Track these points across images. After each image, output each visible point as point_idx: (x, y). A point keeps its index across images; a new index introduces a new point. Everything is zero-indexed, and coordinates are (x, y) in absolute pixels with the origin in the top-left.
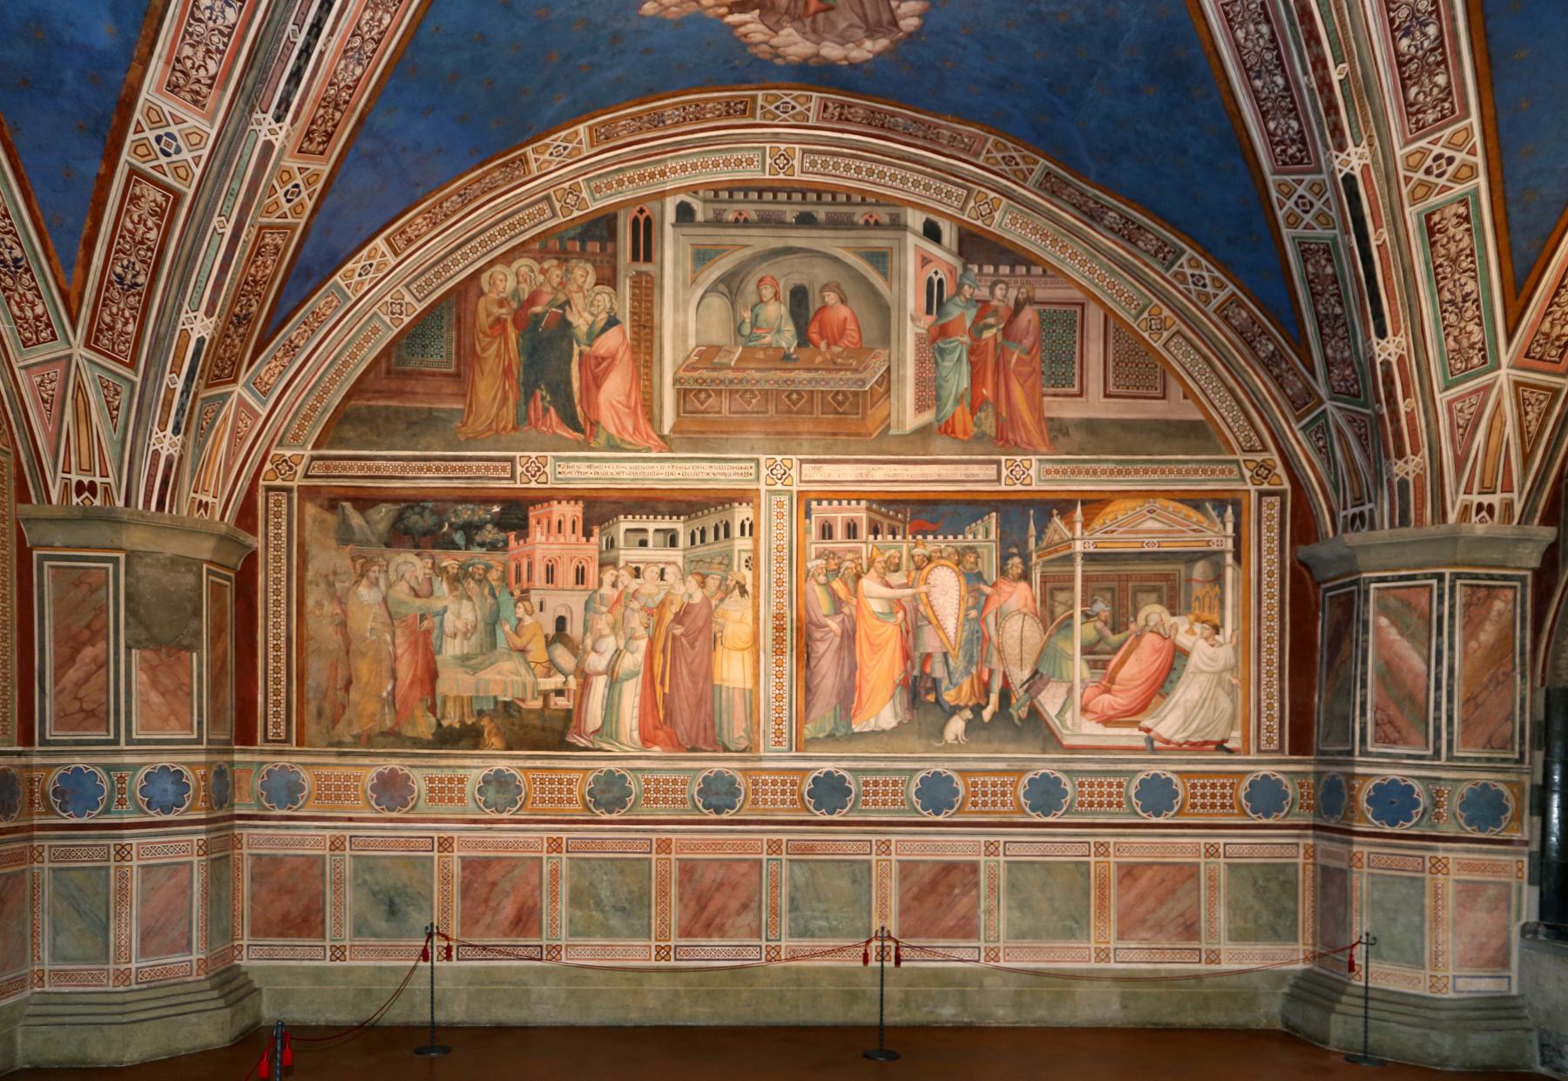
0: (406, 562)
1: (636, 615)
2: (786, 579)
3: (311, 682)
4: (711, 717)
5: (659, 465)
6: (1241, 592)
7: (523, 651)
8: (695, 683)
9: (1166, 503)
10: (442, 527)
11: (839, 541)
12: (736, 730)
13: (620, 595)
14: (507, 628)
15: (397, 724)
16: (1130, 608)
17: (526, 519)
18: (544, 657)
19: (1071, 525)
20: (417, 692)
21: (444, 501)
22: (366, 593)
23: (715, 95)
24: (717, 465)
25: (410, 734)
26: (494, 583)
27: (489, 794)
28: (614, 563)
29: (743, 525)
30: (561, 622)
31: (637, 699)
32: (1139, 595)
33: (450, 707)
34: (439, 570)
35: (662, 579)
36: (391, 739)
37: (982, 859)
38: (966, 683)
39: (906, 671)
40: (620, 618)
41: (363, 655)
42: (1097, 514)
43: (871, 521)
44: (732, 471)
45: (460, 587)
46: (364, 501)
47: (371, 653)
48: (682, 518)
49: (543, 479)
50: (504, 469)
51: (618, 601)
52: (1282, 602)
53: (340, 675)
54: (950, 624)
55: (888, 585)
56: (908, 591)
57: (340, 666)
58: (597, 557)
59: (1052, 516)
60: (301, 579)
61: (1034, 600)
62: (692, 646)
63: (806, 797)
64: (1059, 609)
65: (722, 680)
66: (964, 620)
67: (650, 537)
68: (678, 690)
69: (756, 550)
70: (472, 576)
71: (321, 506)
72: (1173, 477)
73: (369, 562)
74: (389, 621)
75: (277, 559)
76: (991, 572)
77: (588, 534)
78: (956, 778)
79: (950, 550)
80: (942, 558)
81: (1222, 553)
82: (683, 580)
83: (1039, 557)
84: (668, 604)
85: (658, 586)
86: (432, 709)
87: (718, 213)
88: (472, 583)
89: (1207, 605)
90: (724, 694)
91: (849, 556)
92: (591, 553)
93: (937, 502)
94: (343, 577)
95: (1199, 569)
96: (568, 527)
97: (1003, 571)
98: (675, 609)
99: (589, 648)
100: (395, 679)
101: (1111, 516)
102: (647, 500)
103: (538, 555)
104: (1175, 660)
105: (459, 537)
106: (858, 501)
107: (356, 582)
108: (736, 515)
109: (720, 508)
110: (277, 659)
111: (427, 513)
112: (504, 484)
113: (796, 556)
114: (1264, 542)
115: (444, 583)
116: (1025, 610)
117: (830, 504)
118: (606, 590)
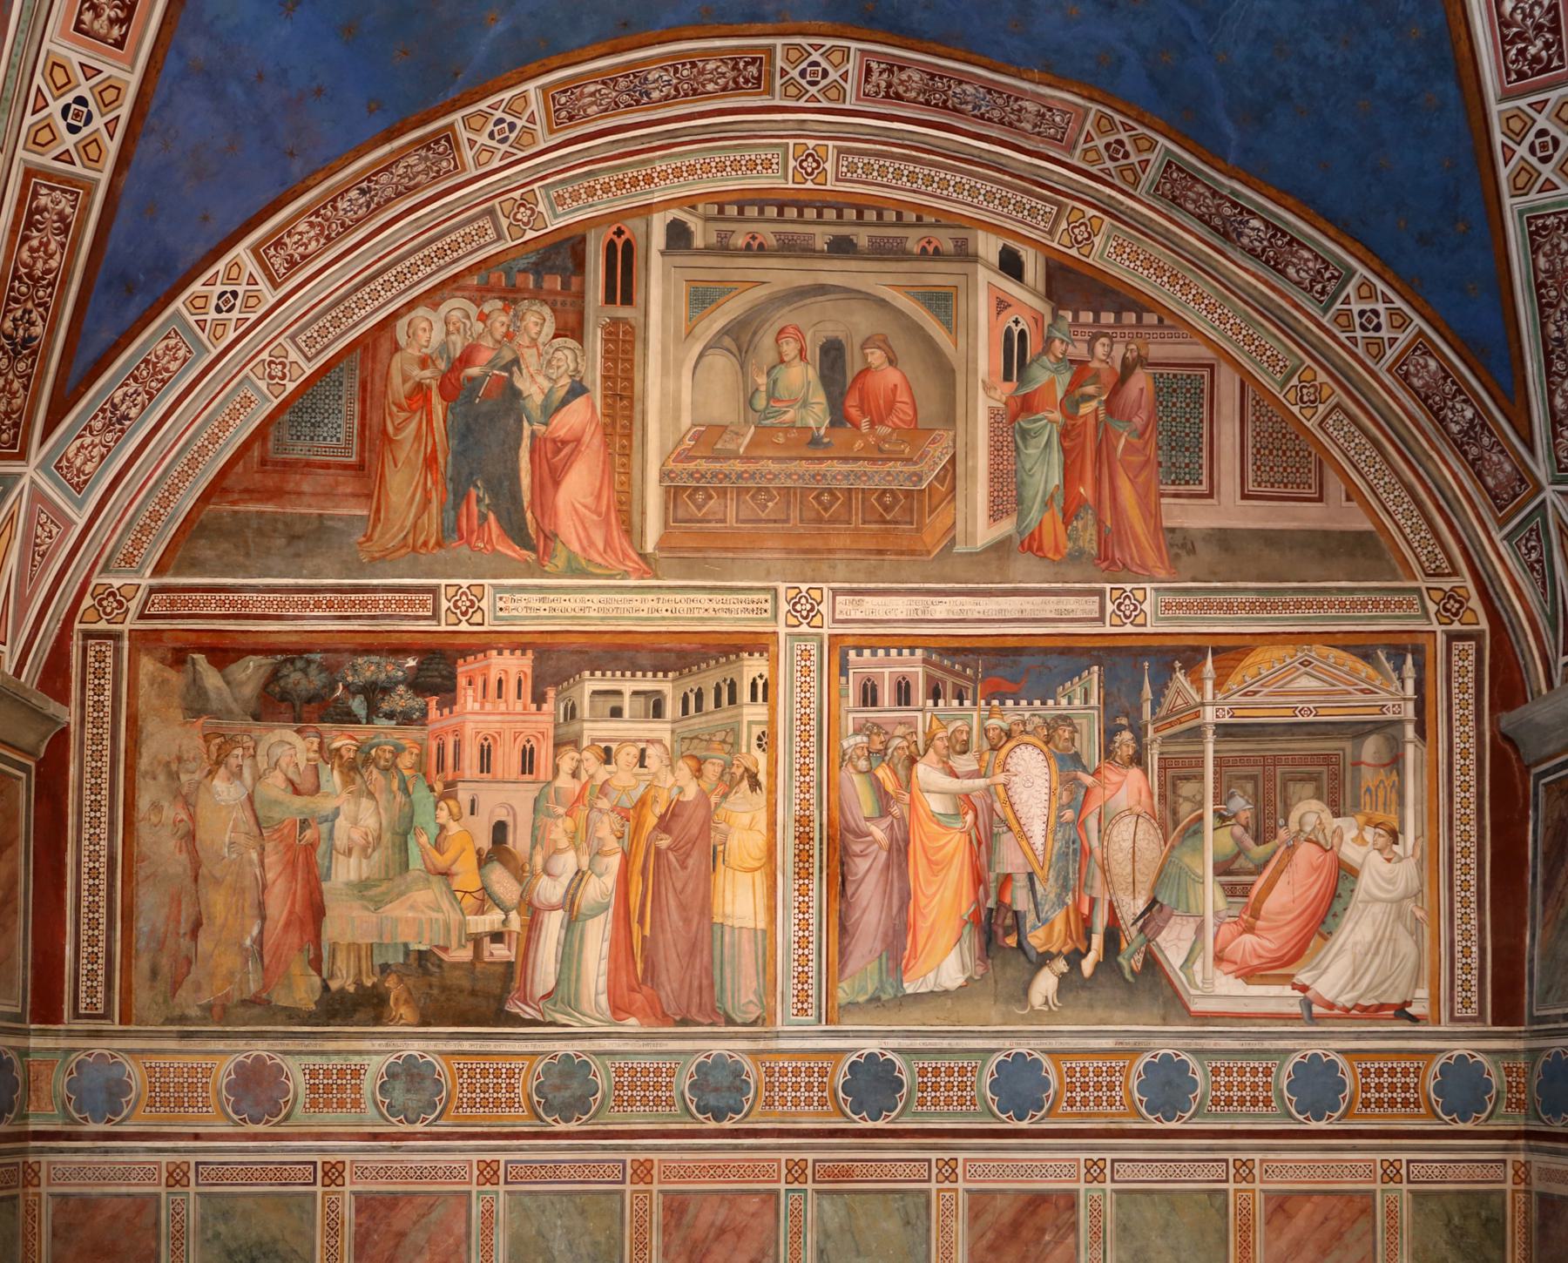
0: (282, 742)
2: (814, 765)
6: (1426, 781)
9: (1325, 650)
11: (887, 710)
12: (743, 993)
13: (583, 788)
16: (1279, 805)
17: (453, 677)
18: (474, 883)
19: (1199, 684)
22: (225, 790)
23: (718, 43)
26: (406, 773)
28: (575, 743)
29: (754, 685)
30: (500, 830)
32: (1291, 787)
34: (328, 754)
35: (642, 766)
37: (1082, 1186)
38: (1059, 917)
39: (977, 900)
41: (218, 882)
42: (1234, 668)
43: (929, 678)
45: (358, 778)
46: (223, 653)
48: (671, 675)
51: (580, 796)
52: (1480, 795)
54: (1037, 831)
55: (953, 774)
56: (980, 783)
58: (551, 733)
59: (1174, 670)
60: (131, 768)
61: (1151, 795)
63: (841, 1094)
64: (1184, 808)
66: (1055, 825)
67: (626, 703)
69: (772, 722)
70: (375, 762)
71: (163, 661)
72: (1333, 613)
73: (228, 743)
74: (255, 830)
75: (97, 739)
76: (1091, 751)
77: (539, 699)
78: (1046, 1062)
79: (1036, 720)
80: (1025, 732)
81: (1400, 723)
82: (672, 766)
83: (1156, 730)
84: (649, 802)
85: (636, 775)
87: (724, 236)
88: (375, 771)
89: (1381, 800)
91: (901, 730)
92: (542, 727)
93: (1018, 651)
94: (192, 766)
95: (1371, 748)
96: (511, 688)
97: (1108, 753)
101: (1253, 671)
103: (469, 729)
104: (1343, 875)
105: (358, 705)
106: (912, 649)
107: (210, 772)
109: (723, 660)
113: (828, 731)
114: (1455, 707)
115: (336, 773)
116: (1138, 809)
117: (874, 654)
118: (564, 781)
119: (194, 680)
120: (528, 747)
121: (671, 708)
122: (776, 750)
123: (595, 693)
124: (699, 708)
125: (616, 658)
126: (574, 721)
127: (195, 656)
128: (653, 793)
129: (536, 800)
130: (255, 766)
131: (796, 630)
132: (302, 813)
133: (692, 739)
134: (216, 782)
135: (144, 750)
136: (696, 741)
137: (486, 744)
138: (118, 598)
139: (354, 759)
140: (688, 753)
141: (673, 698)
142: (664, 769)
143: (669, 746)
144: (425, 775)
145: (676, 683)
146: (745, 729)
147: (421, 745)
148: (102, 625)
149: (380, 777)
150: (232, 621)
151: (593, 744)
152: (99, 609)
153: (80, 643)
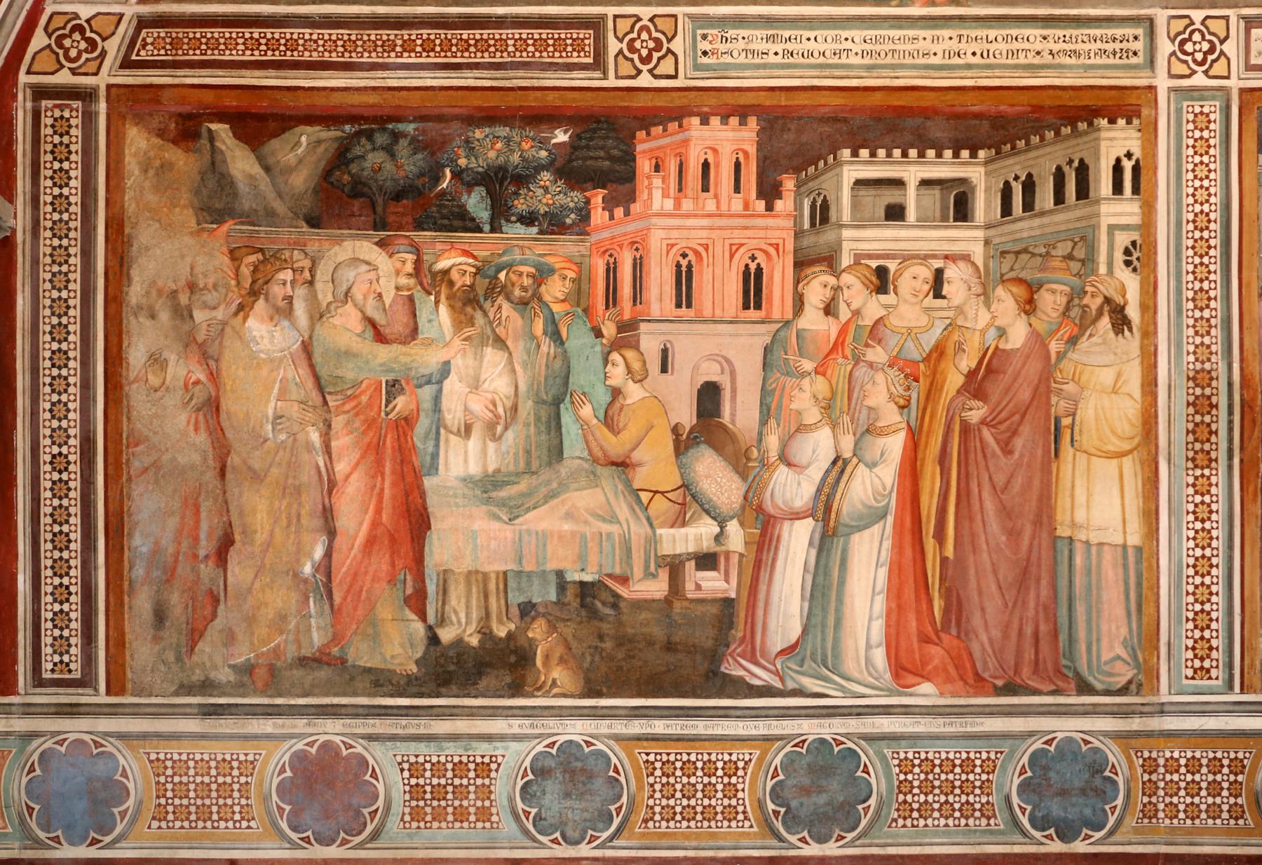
0: (356, 261)
1: (880, 377)
3: (139, 543)
4: (1049, 610)
5: (928, 33)
7: (623, 465)
8: (1013, 534)
10: (437, 179)
13: (843, 331)
14: (586, 411)
15: (336, 638)
17: (629, 158)
20: (380, 563)
21: (440, 118)
24: (1060, 33)
25: (365, 662)
26: (556, 308)
27: (547, 801)
28: (829, 260)
29: (1118, 169)
30: (709, 396)
31: (883, 573)
33: (456, 599)
35: (938, 295)
36: (323, 673)
40: (843, 386)
41: (257, 477)
44: (1099, 45)
45: (478, 316)
47: (275, 471)
48: (982, 154)
49: (667, 67)
50: (579, 47)
51: (838, 345)
53: (204, 526)
57: (206, 505)
58: (790, 246)
60: (115, 301)
62: (1007, 450)
65: (1073, 525)
67: (911, 199)
68: (975, 549)
69: (1147, 226)
70: (506, 292)
71: (161, 134)
73: (270, 261)
74: (315, 397)
75: (60, 256)
77: (769, 192)
82: (986, 295)
84: (950, 351)
85: (928, 310)
86: (417, 601)
90: (1079, 560)
92: (775, 236)
94: (211, 297)
96: (724, 175)
98: (967, 362)
99: (773, 455)
100: (332, 533)
102: (903, 112)
103: (656, 240)
105: (476, 203)
107: (241, 307)
108: (1103, 144)
109: (1066, 131)
110: (61, 489)
111: (403, 147)
112: (579, 79)
115: (443, 309)
118: (812, 320)
119: (213, 163)
120: (753, 267)
121: (984, 205)
122: (1155, 271)
123: (859, 183)
124: (1028, 205)
125: (892, 129)
126: (827, 227)
127: (214, 126)
128: (956, 337)
129: (767, 350)
130: (313, 298)
131: (1185, 83)
132: (391, 370)
133: (1018, 253)
134: (252, 323)
135: (135, 273)
136: (1024, 257)
137: (684, 263)
138: (88, 34)
139: (472, 286)
140: (1012, 275)
141: (987, 190)
142: (974, 300)
143: (980, 264)
144: (585, 311)
145: (992, 167)
146: (1104, 237)
147: (579, 265)
148: (63, 78)
149: (515, 316)
150: (272, 73)
151: (857, 263)
152: (58, 52)
153: (29, 105)
